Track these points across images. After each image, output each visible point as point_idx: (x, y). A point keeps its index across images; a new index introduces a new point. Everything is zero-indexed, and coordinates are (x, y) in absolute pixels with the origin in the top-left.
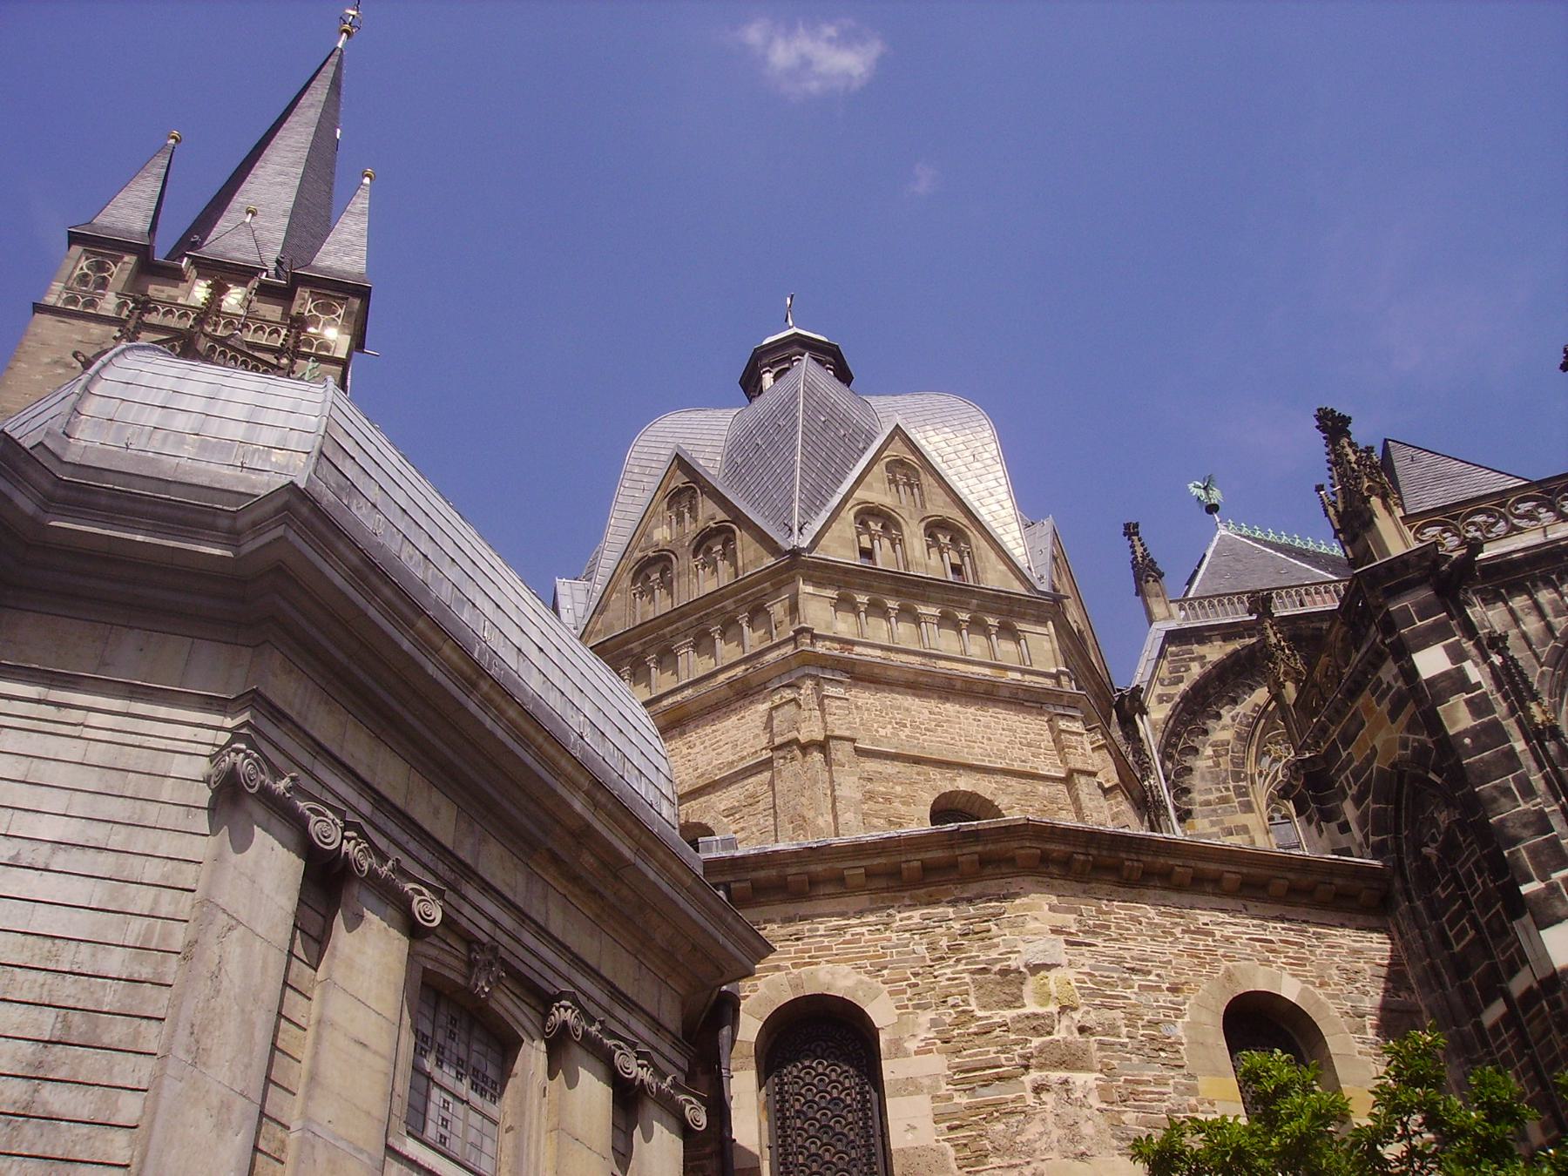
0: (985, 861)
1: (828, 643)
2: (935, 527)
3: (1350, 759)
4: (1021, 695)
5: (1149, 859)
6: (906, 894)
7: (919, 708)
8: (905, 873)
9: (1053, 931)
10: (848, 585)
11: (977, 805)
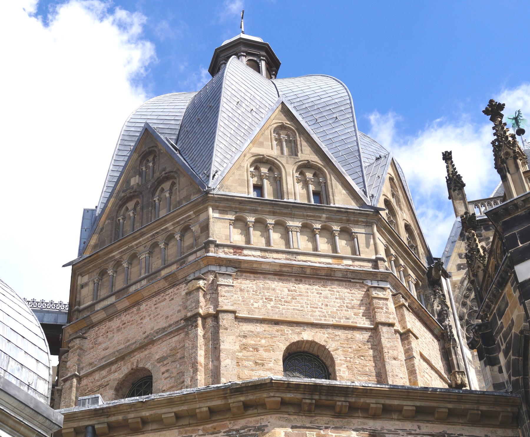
0: (246, 406)
1: (226, 250)
2: (304, 167)
3: (502, 327)
4: (349, 275)
5: (353, 400)
6: (201, 428)
7: (280, 288)
8: (199, 416)
10: (242, 210)
11: (316, 348)
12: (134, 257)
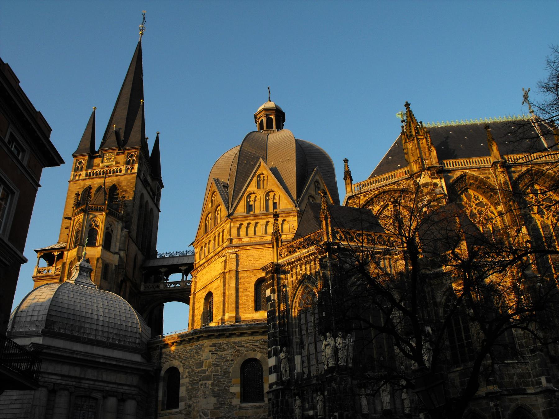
9: (210, 351)
12: (210, 241)
